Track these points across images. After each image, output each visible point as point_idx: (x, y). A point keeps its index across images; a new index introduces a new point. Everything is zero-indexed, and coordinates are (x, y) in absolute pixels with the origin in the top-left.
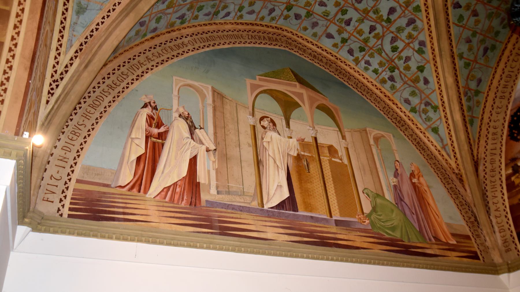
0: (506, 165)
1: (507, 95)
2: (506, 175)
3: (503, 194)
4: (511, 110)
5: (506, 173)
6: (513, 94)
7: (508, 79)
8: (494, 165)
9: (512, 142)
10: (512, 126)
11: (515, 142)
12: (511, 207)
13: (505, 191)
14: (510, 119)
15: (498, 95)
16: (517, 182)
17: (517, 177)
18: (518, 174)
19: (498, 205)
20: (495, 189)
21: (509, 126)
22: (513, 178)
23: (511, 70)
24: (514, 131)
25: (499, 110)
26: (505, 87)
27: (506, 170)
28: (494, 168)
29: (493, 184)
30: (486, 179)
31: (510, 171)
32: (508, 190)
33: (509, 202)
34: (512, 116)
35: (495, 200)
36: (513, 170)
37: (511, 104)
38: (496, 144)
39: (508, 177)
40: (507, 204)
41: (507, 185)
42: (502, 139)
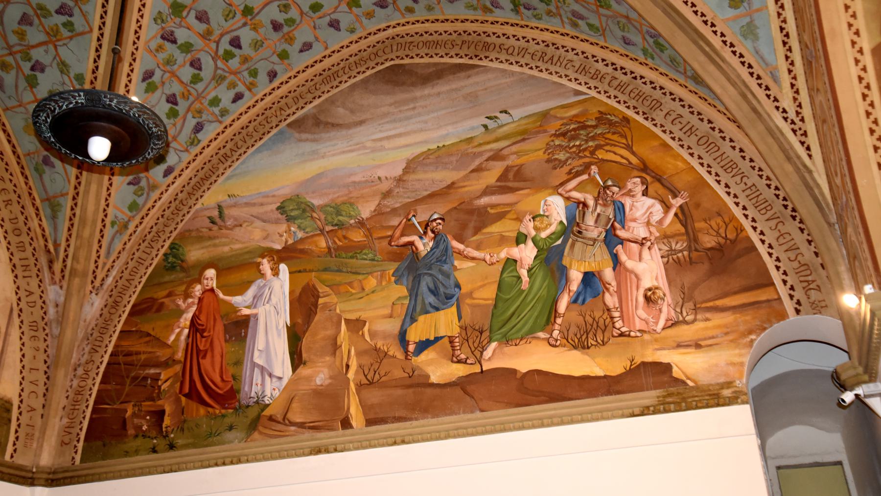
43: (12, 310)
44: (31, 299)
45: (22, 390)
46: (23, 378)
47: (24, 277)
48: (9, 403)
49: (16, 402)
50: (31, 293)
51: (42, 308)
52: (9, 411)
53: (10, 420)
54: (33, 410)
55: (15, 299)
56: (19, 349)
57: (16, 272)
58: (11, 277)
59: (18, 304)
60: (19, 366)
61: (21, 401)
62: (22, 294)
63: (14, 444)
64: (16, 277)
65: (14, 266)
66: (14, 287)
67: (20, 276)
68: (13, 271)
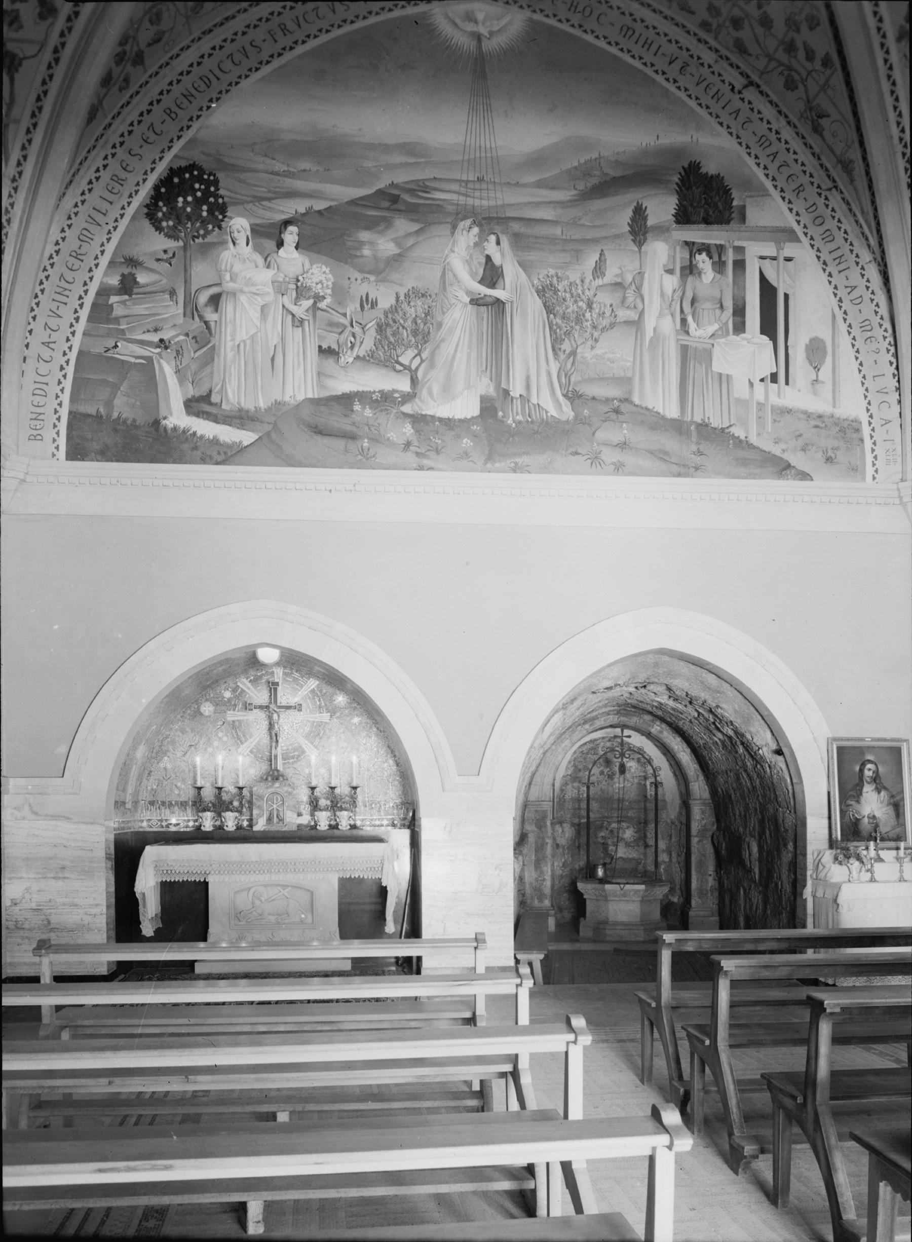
0: (112, 263)
1: (183, 116)
2: (101, 283)
3: (77, 319)
4: (176, 156)
5: (105, 280)
6: (196, 125)
7: (203, 87)
8: (85, 246)
9: (146, 223)
10: (163, 190)
11: (153, 229)
12: (81, 353)
13: (84, 314)
14: (166, 175)
15: (167, 101)
16: (118, 311)
17: (123, 302)
18: (126, 297)
19: (55, 335)
20: (64, 299)
21: (156, 188)
22: (113, 299)
23: (217, 72)
24: (161, 204)
25: (152, 137)
26: (187, 96)
27: (106, 274)
28: (82, 251)
29: (63, 284)
30: (52, 265)
31: (114, 281)
32: (91, 319)
33: (82, 343)
34: (173, 172)
35: (53, 322)
36: (122, 282)
37: (182, 142)
38: (111, 203)
39: (104, 292)
40: (76, 342)
41: (94, 306)
42: (129, 203)
43: (834, 316)
44: (856, 293)
45: (869, 403)
46: (867, 390)
47: (840, 272)
48: (857, 421)
49: (864, 419)
50: (854, 288)
51: (872, 300)
52: (858, 430)
53: (862, 440)
54: (888, 422)
55: (834, 302)
56: (854, 358)
57: (828, 269)
58: (824, 277)
59: (840, 307)
60: (859, 378)
61: (871, 416)
62: (842, 293)
63: (874, 465)
64: (830, 275)
65: (825, 263)
66: (831, 289)
67: (835, 273)
68: (824, 270)
